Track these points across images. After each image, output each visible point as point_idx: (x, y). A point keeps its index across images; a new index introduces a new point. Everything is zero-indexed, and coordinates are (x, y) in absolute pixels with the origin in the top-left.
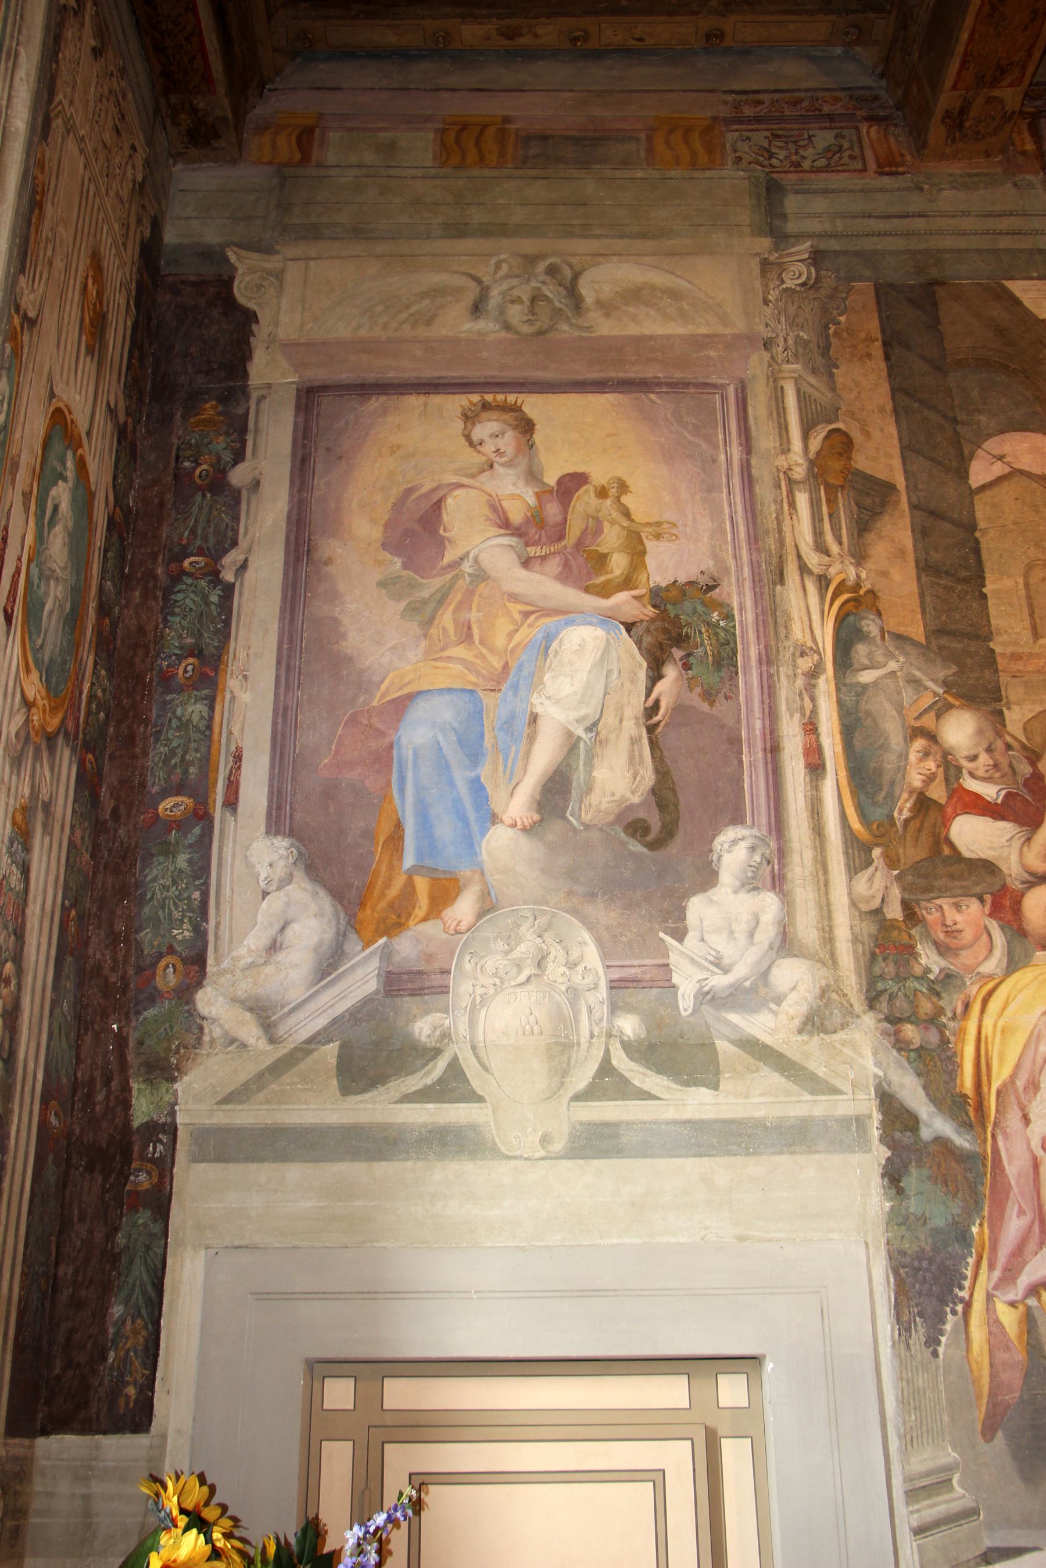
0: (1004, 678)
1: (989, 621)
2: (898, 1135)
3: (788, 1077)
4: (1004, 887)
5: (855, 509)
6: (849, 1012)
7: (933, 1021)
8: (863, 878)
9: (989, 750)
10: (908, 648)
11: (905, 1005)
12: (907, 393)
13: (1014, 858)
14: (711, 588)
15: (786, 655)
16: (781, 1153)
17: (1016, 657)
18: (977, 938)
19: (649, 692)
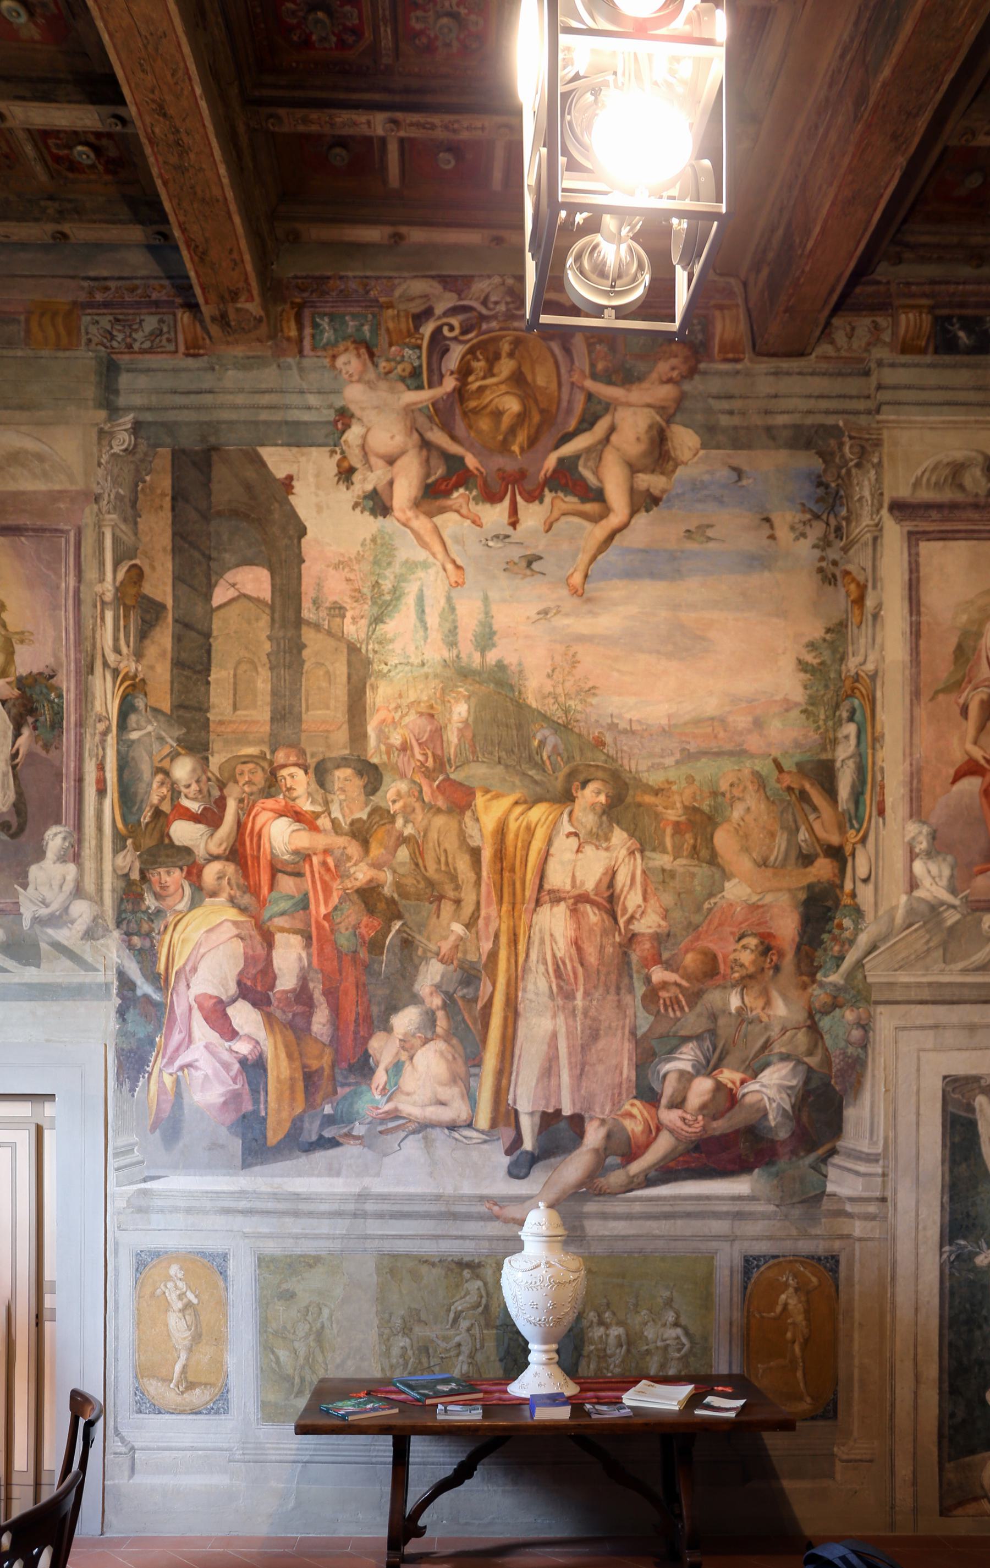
0: (212, 736)
4: (194, 862)
6: (107, 930)
7: (148, 935)
8: (120, 856)
9: (198, 781)
10: (161, 718)
13: (202, 846)
14: (51, 677)
15: (91, 721)
17: (221, 723)
18: (176, 891)
19: (14, 743)
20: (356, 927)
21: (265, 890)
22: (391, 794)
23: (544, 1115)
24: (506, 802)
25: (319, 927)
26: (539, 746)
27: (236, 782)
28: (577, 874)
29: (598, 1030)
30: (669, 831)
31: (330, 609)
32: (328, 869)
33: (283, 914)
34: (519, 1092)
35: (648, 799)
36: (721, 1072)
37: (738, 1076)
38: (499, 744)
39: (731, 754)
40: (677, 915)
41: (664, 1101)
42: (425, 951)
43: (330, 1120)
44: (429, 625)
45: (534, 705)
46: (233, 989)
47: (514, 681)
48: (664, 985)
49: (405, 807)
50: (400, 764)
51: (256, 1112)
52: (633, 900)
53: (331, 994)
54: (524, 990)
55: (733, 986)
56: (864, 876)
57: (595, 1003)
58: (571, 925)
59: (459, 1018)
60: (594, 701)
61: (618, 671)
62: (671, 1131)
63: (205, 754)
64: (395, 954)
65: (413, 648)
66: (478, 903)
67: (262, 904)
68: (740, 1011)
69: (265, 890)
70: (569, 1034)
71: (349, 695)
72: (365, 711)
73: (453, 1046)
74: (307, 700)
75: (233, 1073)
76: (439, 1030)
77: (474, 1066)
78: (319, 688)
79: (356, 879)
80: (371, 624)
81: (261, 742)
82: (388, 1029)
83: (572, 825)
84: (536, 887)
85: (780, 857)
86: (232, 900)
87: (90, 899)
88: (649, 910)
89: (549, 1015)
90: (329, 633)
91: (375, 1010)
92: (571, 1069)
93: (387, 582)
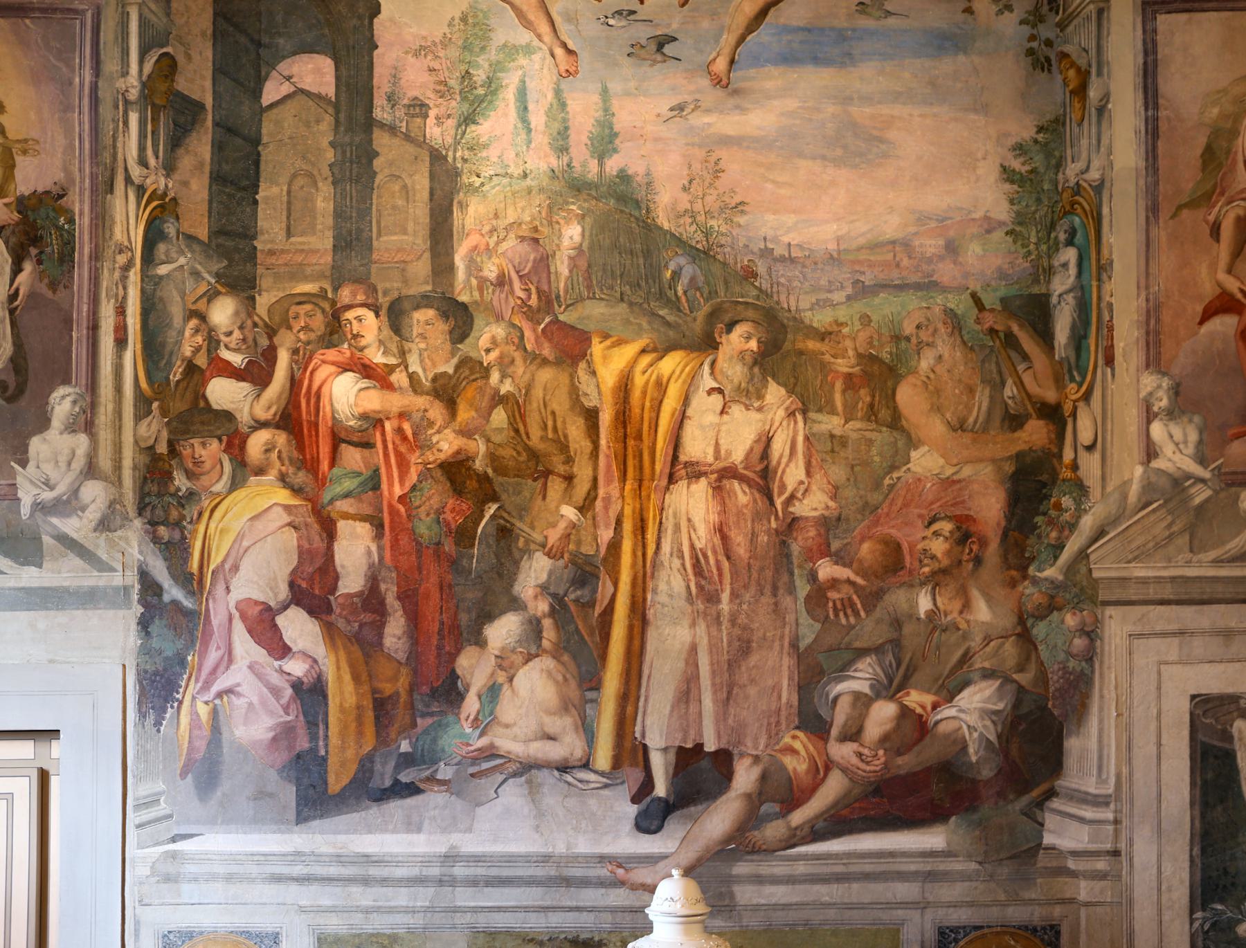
0: (260, 270)
1: (256, 223)
2: (149, 598)
3: (85, 561)
4: (237, 431)
5: (172, 126)
7: (178, 524)
9: (241, 328)
10: (196, 247)
11: (162, 513)
12: (225, 18)
13: (246, 410)
14: (61, 197)
15: (109, 253)
16: (78, 609)
17: (272, 253)
18: (213, 467)
20: (440, 512)
21: (325, 465)
22: (484, 342)
23: (681, 751)
24: (630, 350)
25: (393, 512)
26: (673, 278)
27: (290, 328)
28: (722, 442)
29: (749, 642)
30: (839, 385)
31: (410, 106)
32: (404, 438)
33: (347, 495)
34: (648, 722)
35: (812, 345)
36: (908, 694)
37: (928, 699)
38: (621, 276)
39: (918, 287)
40: (849, 493)
41: (834, 732)
42: (527, 542)
43: (408, 761)
44: (533, 126)
45: (666, 226)
46: (284, 592)
47: (641, 194)
48: (834, 583)
49: (501, 357)
50: (495, 303)
51: (313, 751)
52: (794, 474)
53: (408, 597)
54: (655, 591)
55: (923, 584)
57: (745, 607)
58: (714, 507)
59: (572, 628)
60: (742, 220)
61: (774, 182)
63: (251, 292)
64: (489, 546)
65: (513, 155)
67: (321, 482)
68: (931, 615)
69: (325, 465)
70: (713, 648)
71: (432, 216)
72: (452, 236)
73: (563, 664)
74: (379, 222)
75: (284, 701)
76: (545, 643)
77: (591, 689)
78: (394, 207)
79: (440, 450)
80: (459, 125)
81: (320, 276)
82: (481, 643)
83: (715, 379)
84: (669, 458)
85: (981, 419)
86: (283, 479)
87: (106, 479)
88: (814, 488)
89: (686, 622)
90: (407, 137)
91: (464, 618)
92: (715, 693)
93: (480, 72)
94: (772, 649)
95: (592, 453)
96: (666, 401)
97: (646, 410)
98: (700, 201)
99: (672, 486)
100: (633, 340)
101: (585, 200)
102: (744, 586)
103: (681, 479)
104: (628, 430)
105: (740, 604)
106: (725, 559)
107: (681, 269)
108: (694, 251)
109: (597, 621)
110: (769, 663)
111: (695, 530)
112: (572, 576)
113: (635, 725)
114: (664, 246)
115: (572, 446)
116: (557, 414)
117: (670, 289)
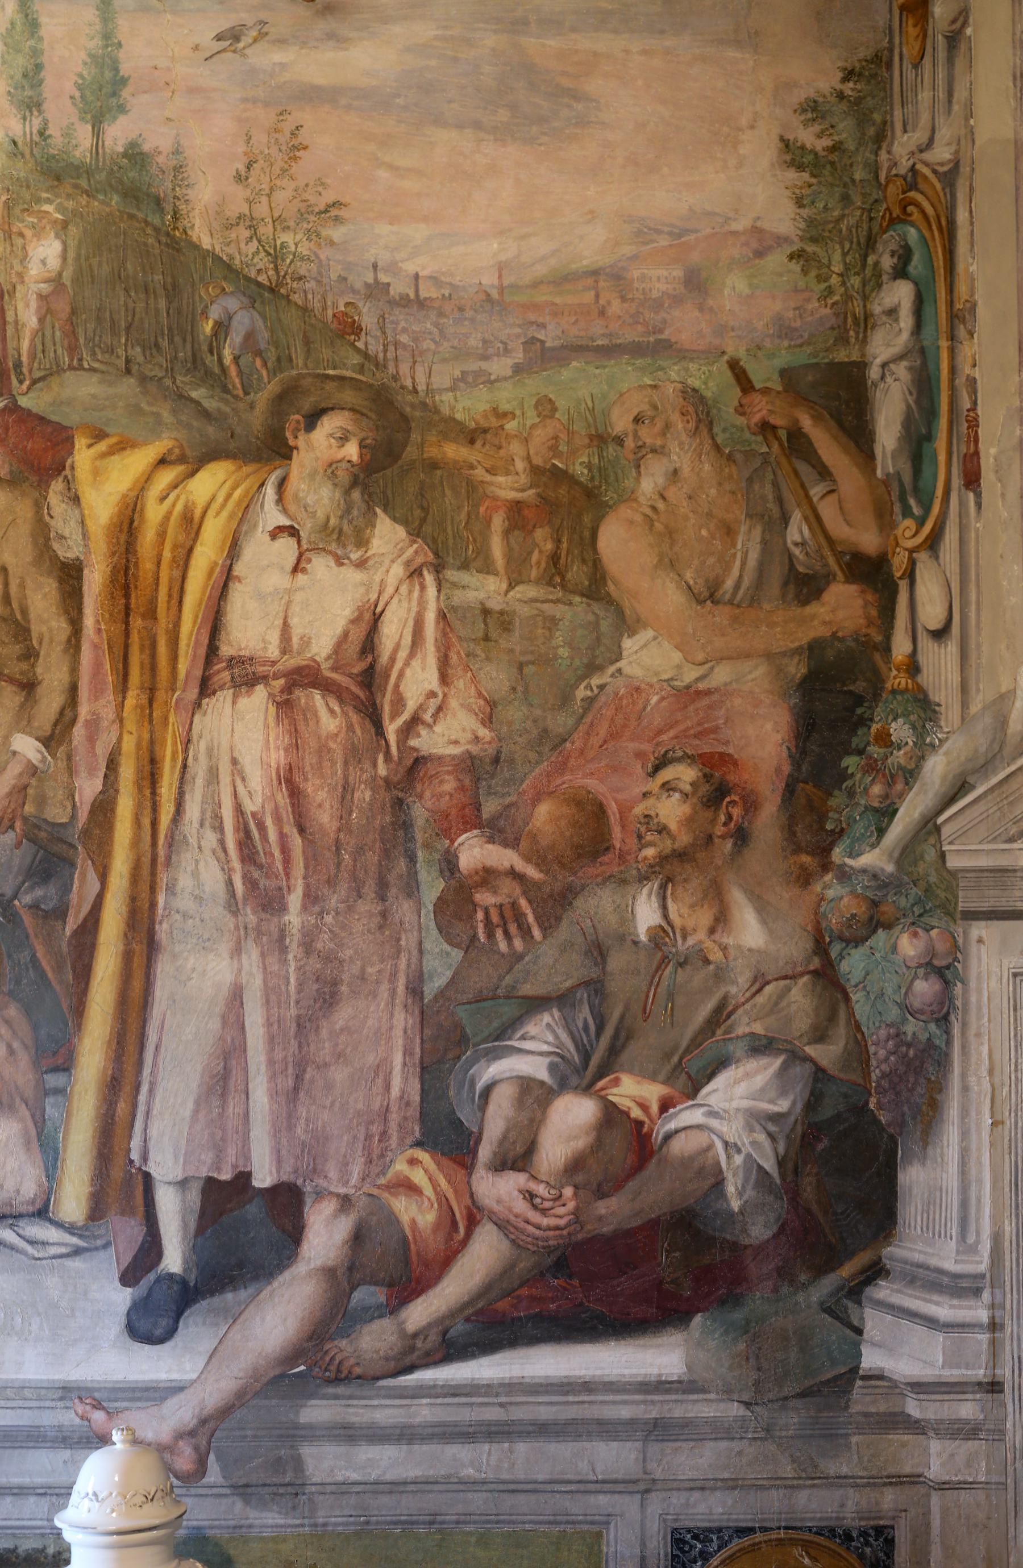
23: (211, 1185)
24: (140, 460)
26: (215, 334)
28: (294, 621)
29: (335, 983)
30: (498, 522)
34: (154, 1132)
35: (453, 451)
36: (616, 1082)
37: (653, 1092)
38: (128, 329)
39: (636, 350)
40: (515, 713)
41: (485, 1152)
45: (206, 243)
47: (164, 187)
48: (487, 876)
54: (171, 890)
55: (643, 879)
56: (935, 625)
57: (329, 919)
59: (25, 956)
60: (337, 233)
61: (391, 167)
62: (502, 1225)
66: (73, 690)
68: (660, 935)
70: (271, 994)
77: (56, 1069)
83: (285, 511)
84: (202, 651)
85: (746, 582)
88: (453, 703)
89: (225, 947)
92: (273, 1077)
94: (375, 997)
95: (69, 641)
96: (198, 550)
97: (164, 566)
98: (264, 199)
99: (205, 701)
100: (145, 443)
101: (69, 196)
102: (328, 882)
103: (222, 688)
104: (133, 601)
105: (321, 914)
106: (295, 831)
107: (230, 318)
108: (253, 287)
109: (69, 944)
110: (370, 1022)
111: (243, 780)
112: (28, 860)
113: (130, 1137)
114: (202, 279)
115: (35, 628)
116: (10, 572)
117: (211, 353)
